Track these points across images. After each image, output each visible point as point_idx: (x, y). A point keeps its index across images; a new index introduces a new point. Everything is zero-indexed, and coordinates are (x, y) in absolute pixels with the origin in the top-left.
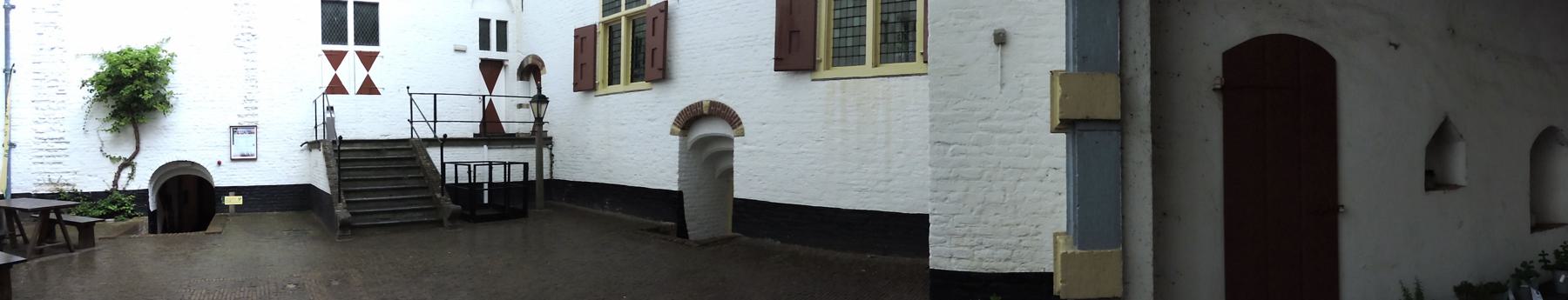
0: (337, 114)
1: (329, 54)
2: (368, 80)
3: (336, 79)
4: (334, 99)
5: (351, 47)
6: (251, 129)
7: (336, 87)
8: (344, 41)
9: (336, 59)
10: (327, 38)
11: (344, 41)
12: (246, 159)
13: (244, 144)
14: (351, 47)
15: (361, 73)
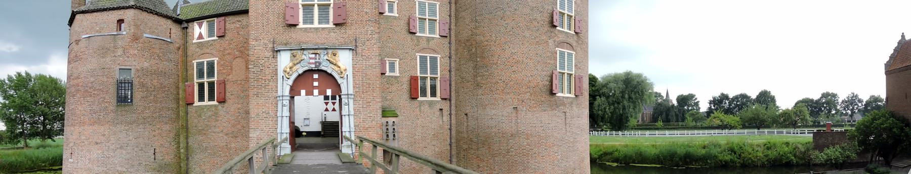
0: (327, 116)
1: (325, 103)
2: (334, 108)
3: (327, 108)
4: (326, 113)
5: (330, 101)
6: (308, 119)
7: (327, 110)
8: (329, 100)
9: (327, 104)
10: (325, 100)
11: (329, 100)
12: (307, 125)
13: (307, 122)
14: (330, 101)
15: (332, 107)
